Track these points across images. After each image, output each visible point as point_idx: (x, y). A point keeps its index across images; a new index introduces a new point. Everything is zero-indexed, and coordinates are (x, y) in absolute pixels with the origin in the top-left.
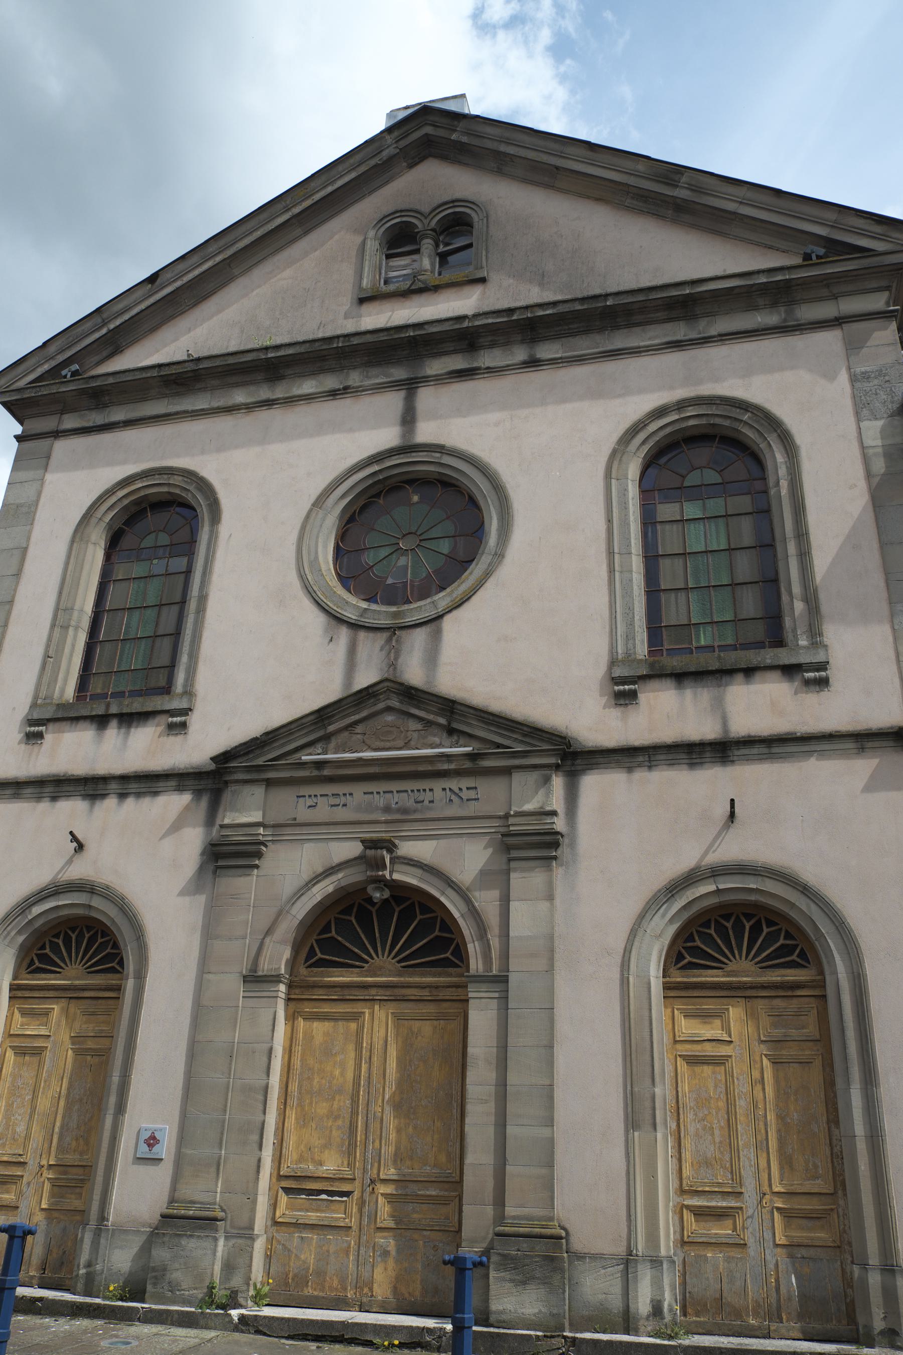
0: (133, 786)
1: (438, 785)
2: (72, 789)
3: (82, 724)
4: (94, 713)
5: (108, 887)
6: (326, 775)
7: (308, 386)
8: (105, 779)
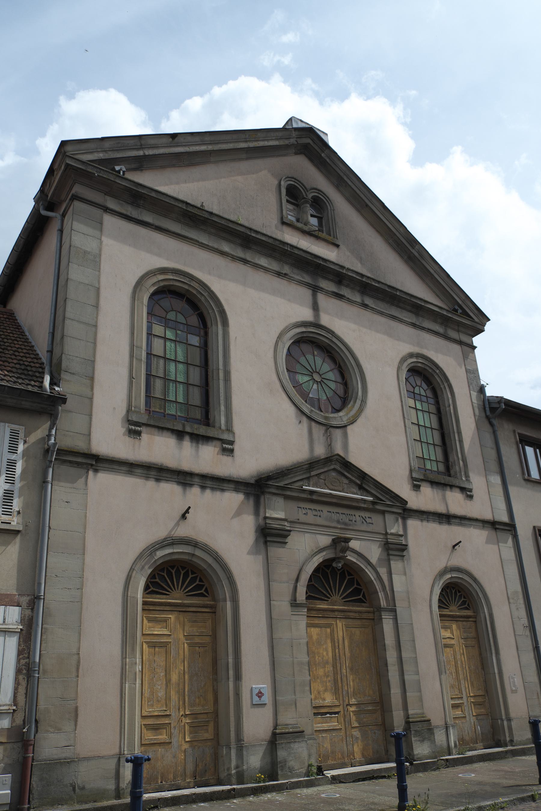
0: (209, 483)
1: (358, 513)
2: (168, 476)
3: (165, 433)
4: (176, 428)
5: (206, 545)
6: (313, 499)
7: (263, 261)
8: (191, 474)
